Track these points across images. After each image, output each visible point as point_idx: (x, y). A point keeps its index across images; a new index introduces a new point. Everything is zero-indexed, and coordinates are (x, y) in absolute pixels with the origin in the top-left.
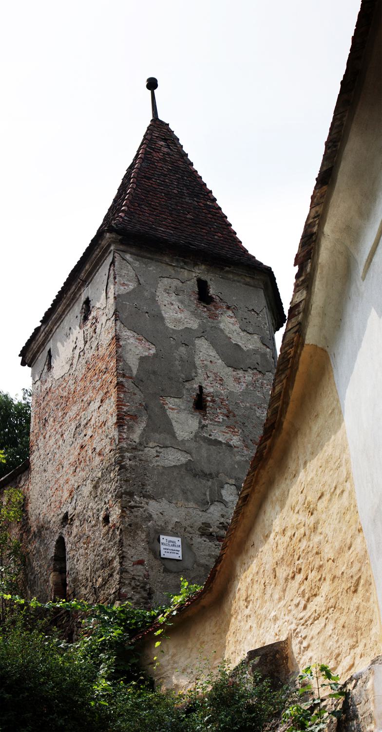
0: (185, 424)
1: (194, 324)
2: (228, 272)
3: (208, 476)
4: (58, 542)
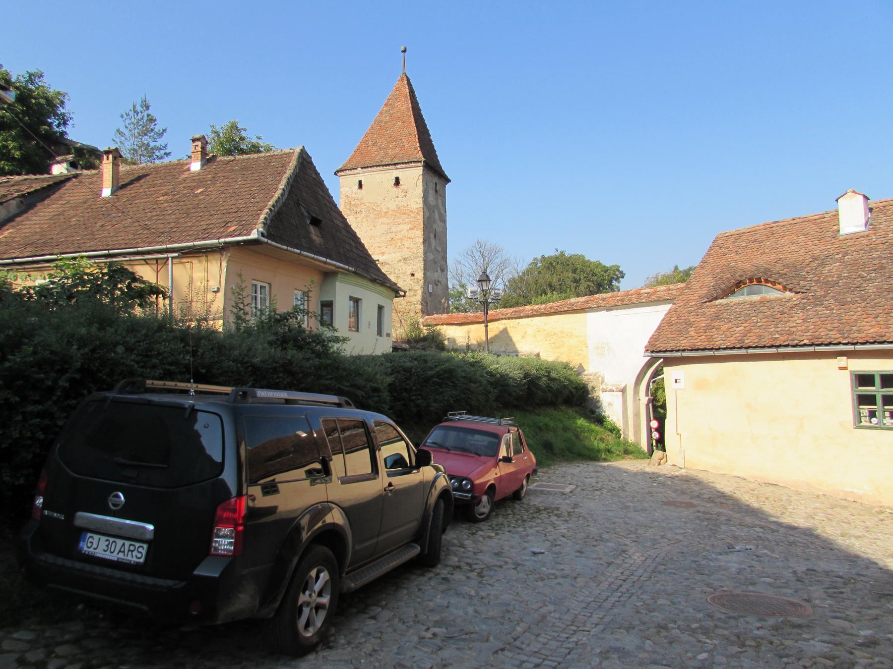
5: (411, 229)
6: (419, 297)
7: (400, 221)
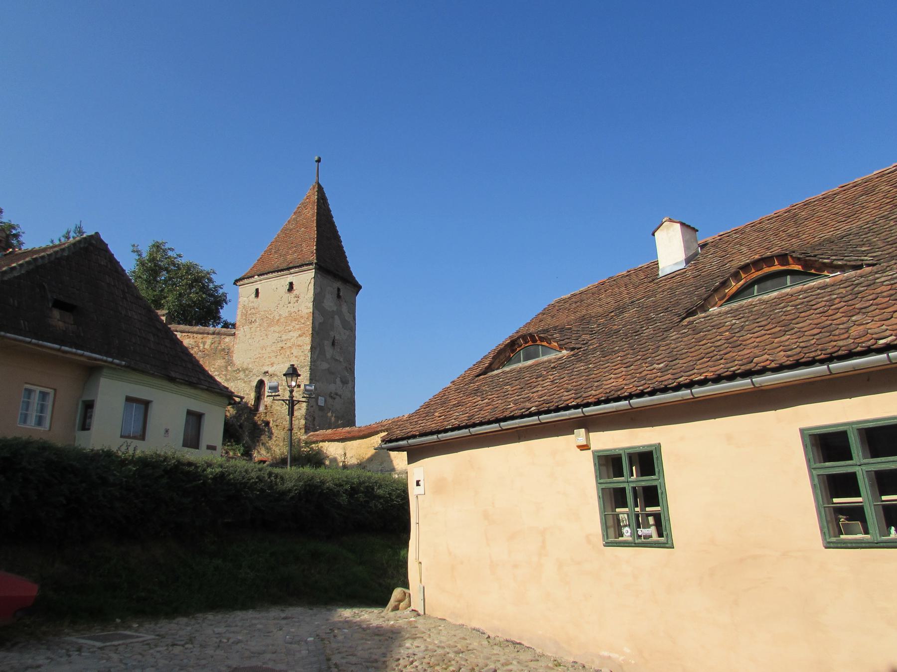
5: (300, 336)
7: (290, 328)
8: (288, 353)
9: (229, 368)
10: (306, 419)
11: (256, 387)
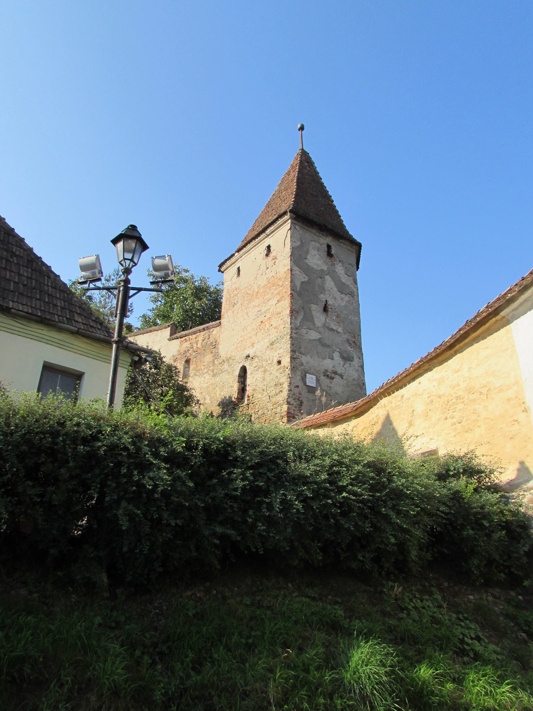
0: (320, 318)
1: (325, 268)
2: (341, 242)
3: (328, 346)
4: (241, 368)
6: (285, 394)
8: (268, 326)
9: (216, 362)
10: (288, 403)
11: (240, 376)
